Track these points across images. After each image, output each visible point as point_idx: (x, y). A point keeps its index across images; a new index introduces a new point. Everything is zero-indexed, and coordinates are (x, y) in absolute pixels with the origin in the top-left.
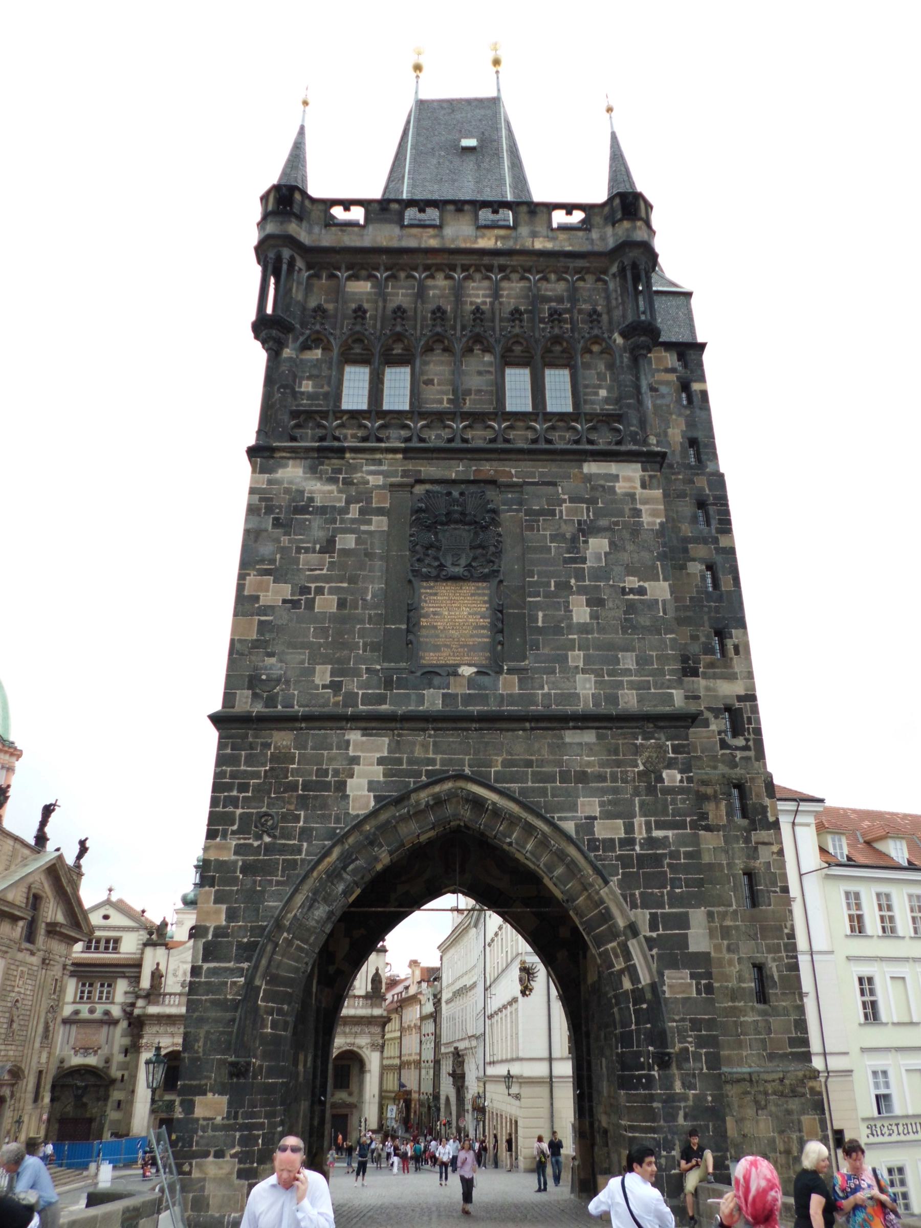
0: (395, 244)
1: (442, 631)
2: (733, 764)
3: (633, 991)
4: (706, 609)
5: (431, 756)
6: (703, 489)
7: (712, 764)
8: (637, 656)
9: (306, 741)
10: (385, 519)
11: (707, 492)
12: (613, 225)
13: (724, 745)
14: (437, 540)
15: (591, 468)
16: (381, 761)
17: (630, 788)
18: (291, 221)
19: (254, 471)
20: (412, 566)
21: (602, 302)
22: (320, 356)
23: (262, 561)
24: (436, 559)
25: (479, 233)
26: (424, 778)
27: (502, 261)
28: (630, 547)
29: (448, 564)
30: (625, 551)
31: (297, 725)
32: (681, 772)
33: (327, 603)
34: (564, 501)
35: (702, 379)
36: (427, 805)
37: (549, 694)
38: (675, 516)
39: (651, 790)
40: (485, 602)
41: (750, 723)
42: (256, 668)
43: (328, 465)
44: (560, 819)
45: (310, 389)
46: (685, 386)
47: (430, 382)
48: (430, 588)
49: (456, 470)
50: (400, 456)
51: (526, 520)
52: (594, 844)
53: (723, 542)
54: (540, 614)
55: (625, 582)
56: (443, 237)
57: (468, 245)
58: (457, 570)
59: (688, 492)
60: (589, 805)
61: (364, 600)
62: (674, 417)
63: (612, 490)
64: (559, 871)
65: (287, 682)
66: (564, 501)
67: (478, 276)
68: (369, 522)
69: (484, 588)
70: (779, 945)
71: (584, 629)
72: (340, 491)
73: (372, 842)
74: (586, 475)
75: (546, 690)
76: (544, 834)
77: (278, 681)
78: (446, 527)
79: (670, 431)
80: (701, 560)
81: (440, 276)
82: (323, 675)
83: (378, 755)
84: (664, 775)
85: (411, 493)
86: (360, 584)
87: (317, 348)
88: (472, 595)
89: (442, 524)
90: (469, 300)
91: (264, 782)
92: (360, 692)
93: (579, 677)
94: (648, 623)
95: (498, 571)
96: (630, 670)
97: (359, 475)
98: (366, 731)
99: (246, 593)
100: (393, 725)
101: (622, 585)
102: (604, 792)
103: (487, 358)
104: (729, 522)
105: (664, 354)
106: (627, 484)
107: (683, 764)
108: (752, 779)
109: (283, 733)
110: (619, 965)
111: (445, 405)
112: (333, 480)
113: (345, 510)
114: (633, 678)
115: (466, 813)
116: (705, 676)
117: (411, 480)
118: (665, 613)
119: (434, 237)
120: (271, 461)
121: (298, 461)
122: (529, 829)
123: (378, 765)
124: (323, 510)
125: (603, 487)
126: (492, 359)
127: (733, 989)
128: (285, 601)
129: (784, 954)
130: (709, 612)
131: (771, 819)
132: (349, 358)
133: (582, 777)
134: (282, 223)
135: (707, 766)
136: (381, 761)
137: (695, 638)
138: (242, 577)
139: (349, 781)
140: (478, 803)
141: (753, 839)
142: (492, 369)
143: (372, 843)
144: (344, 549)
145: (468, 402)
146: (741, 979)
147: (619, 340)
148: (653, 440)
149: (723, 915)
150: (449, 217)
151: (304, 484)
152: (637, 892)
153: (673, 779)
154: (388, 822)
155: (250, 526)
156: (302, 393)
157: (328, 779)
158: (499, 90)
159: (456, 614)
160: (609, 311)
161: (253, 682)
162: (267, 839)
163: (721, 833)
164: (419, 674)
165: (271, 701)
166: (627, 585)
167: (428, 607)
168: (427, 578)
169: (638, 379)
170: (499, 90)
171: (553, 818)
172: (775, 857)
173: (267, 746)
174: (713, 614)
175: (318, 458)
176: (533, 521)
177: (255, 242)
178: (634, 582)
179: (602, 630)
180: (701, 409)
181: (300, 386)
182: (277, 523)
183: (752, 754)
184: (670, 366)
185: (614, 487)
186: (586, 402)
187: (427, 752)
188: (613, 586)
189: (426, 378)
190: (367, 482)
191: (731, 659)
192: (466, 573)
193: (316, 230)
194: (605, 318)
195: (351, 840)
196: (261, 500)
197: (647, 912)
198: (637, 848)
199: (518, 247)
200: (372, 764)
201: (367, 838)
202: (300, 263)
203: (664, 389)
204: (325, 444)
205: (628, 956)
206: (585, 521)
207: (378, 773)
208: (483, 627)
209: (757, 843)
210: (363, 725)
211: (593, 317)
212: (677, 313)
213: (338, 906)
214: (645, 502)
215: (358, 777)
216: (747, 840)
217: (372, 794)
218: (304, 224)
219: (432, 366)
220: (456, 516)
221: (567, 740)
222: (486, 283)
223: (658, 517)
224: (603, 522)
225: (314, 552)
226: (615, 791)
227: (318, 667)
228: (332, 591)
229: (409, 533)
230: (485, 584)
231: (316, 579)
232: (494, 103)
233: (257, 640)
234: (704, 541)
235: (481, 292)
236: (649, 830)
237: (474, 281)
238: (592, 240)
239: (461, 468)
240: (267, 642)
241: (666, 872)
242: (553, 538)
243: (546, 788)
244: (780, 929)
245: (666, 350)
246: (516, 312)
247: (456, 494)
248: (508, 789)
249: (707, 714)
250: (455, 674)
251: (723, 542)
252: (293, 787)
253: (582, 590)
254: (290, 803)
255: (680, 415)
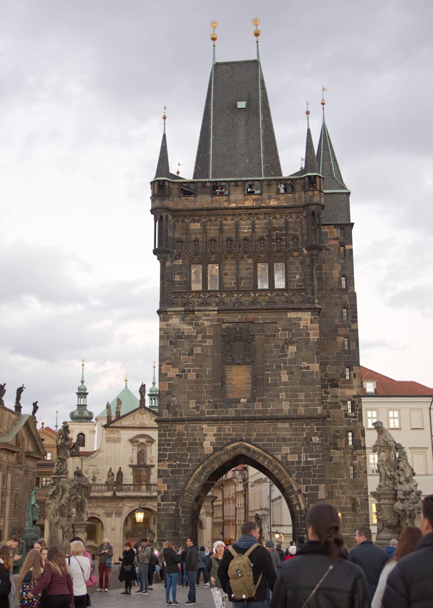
0: (210, 206)
1: (234, 385)
2: (350, 424)
3: (300, 511)
4: (343, 358)
5: (231, 433)
6: (346, 301)
7: (341, 424)
8: (305, 394)
9: (188, 428)
10: (211, 340)
11: (348, 302)
12: (305, 192)
13: (346, 416)
14: (231, 348)
15: (291, 315)
16: (214, 435)
17: (300, 443)
18: (165, 199)
19: (160, 321)
20: (222, 359)
21: (299, 229)
22: (181, 263)
23: (167, 359)
24: (232, 356)
25: (245, 198)
26: (229, 441)
27: (256, 211)
28: (304, 350)
29: (236, 359)
30: (303, 351)
31: (185, 422)
32: (319, 438)
33: (192, 376)
34: (280, 330)
35: (351, 243)
36: (231, 450)
37: (272, 409)
38: (333, 315)
39: (308, 444)
40: (250, 373)
41: (357, 407)
42: (169, 402)
43: (189, 317)
44: (276, 454)
45: (179, 280)
46: (343, 245)
47: (226, 274)
48: (229, 368)
49: (238, 317)
50: (216, 312)
51: (265, 339)
52: (287, 463)
53: (353, 327)
54: (270, 378)
55: (302, 364)
56: (230, 201)
57: (241, 205)
58: (239, 361)
59: (339, 303)
60: (286, 449)
61: (205, 374)
62: (336, 264)
63: (299, 325)
64: (276, 471)
65: (180, 407)
66: (280, 330)
67: (246, 218)
68: (206, 342)
69: (249, 368)
70: (361, 492)
71: (286, 384)
72: (194, 329)
73: (212, 462)
74: (288, 318)
75: (271, 408)
76: (270, 460)
77: (177, 406)
78: (234, 343)
79: (334, 272)
80: (343, 336)
81: (229, 218)
82: (192, 404)
83: (213, 433)
84: (313, 439)
85: (221, 328)
86: (204, 368)
87: (180, 259)
88: (245, 370)
89: (233, 342)
90: (242, 231)
91: (175, 443)
92: (206, 410)
93: (284, 402)
94: (310, 381)
95: (254, 361)
96: (302, 400)
97: (201, 321)
98: (209, 425)
99: (162, 372)
100: (218, 422)
101: (301, 366)
102: (291, 445)
103: (250, 261)
104: (356, 317)
105: (334, 230)
106: (305, 322)
107: (320, 434)
108: (356, 430)
109: (180, 425)
110: (295, 502)
111: (233, 285)
112: (191, 324)
113: (196, 337)
114: (304, 403)
115: (244, 452)
116: (341, 387)
117: (220, 323)
118: (316, 377)
119: (226, 201)
120: (167, 316)
121: (177, 315)
122: (265, 458)
123: (214, 436)
124: (188, 337)
125: (295, 323)
126: (252, 262)
127: (343, 507)
128: (177, 375)
129: (363, 495)
130: (344, 359)
131: (363, 445)
132: (192, 262)
133: (284, 440)
134: (162, 200)
135: (339, 424)
136: (214, 435)
137: (337, 371)
138: (160, 366)
139: (204, 442)
140: (248, 449)
141: (354, 453)
142: (252, 267)
143: (212, 463)
144: (196, 354)
145: (242, 283)
146: (346, 504)
147: (305, 252)
148: (316, 301)
149: (341, 481)
150: (232, 189)
151: (180, 326)
152: (301, 479)
153: (316, 440)
154: (218, 456)
155: (161, 345)
156: (176, 281)
157: (197, 441)
158: (258, 56)
159: (239, 377)
160: (302, 235)
161: (168, 407)
162: (178, 462)
163: (342, 451)
164: (226, 402)
165: (175, 414)
166: (302, 366)
167: (229, 376)
168: (228, 364)
169: (312, 270)
170: (258, 56)
171: (273, 454)
172: (363, 460)
173: (175, 430)
174: (346, 360)
175: (185, 314)
176: (268, 340)
177: (150, 208)
178: (305, 364)
179: (292, 384)
180: (349, 259)
181: (175, 279)
182: (171, 343)
183: (357, 419)
184: (336, 236)
185: (300, 323)
186: (290, 281)
187: (230, 431)
188: (297, 366)
189: (225, 272)
190: (204, 325)
191: (352, 380)
192: (242, 362)
193: (176, 199)
194: (300, 237)
195: (206, 462)
196: (164, 333)
197: (305, 486)
198: (302, 464)
199: (263, 205)
200: (211, 436)
201: (211, 462)
202: (170, 218)
203: (332, 249)
204: (188, 308)
205: (298, 500)
206: (288, 339)
207: (213, 439)
208: (249, 383)
209: (357, 454)
210: (208, 422)
211: (295, 237)
212: (342, 205)
213: (202, 483)
214: (312, 329)
215: (207, 441)
216: (352, 454)
217: (212, 447)
218: (171, 197)
219: (227, 266)
220: (239, 339)
221: (279, 426)
222: (249, 222)
223: (316, 336)
224: (295, 339)
225: (186, 355)
226: (295, 444)
227: (190, 401)
228: (194, 371)
229: (221, 345)
230: (249, 366)
231: (187, 366)
232: (256, 63)
233: (169, 391)
234: (345, 327)
235: (247, 227)
236: (306, 458)
237: (244, 221)
238: (296, 199)
239: (240, 317)
240: (172, 391)
241: (311, 473)
242: (275, 347)
243: (271, 444)
244: (362, 486)
245: (335, 228)
246: (262, 239)
247: (238, 329)
248: (258, 444)
249: (341, 404)
250: (240, 403)
251: (353, 327)
252: (185, 444)
253: (285, 368)
254: (184, 450)
255: (339, 263)
